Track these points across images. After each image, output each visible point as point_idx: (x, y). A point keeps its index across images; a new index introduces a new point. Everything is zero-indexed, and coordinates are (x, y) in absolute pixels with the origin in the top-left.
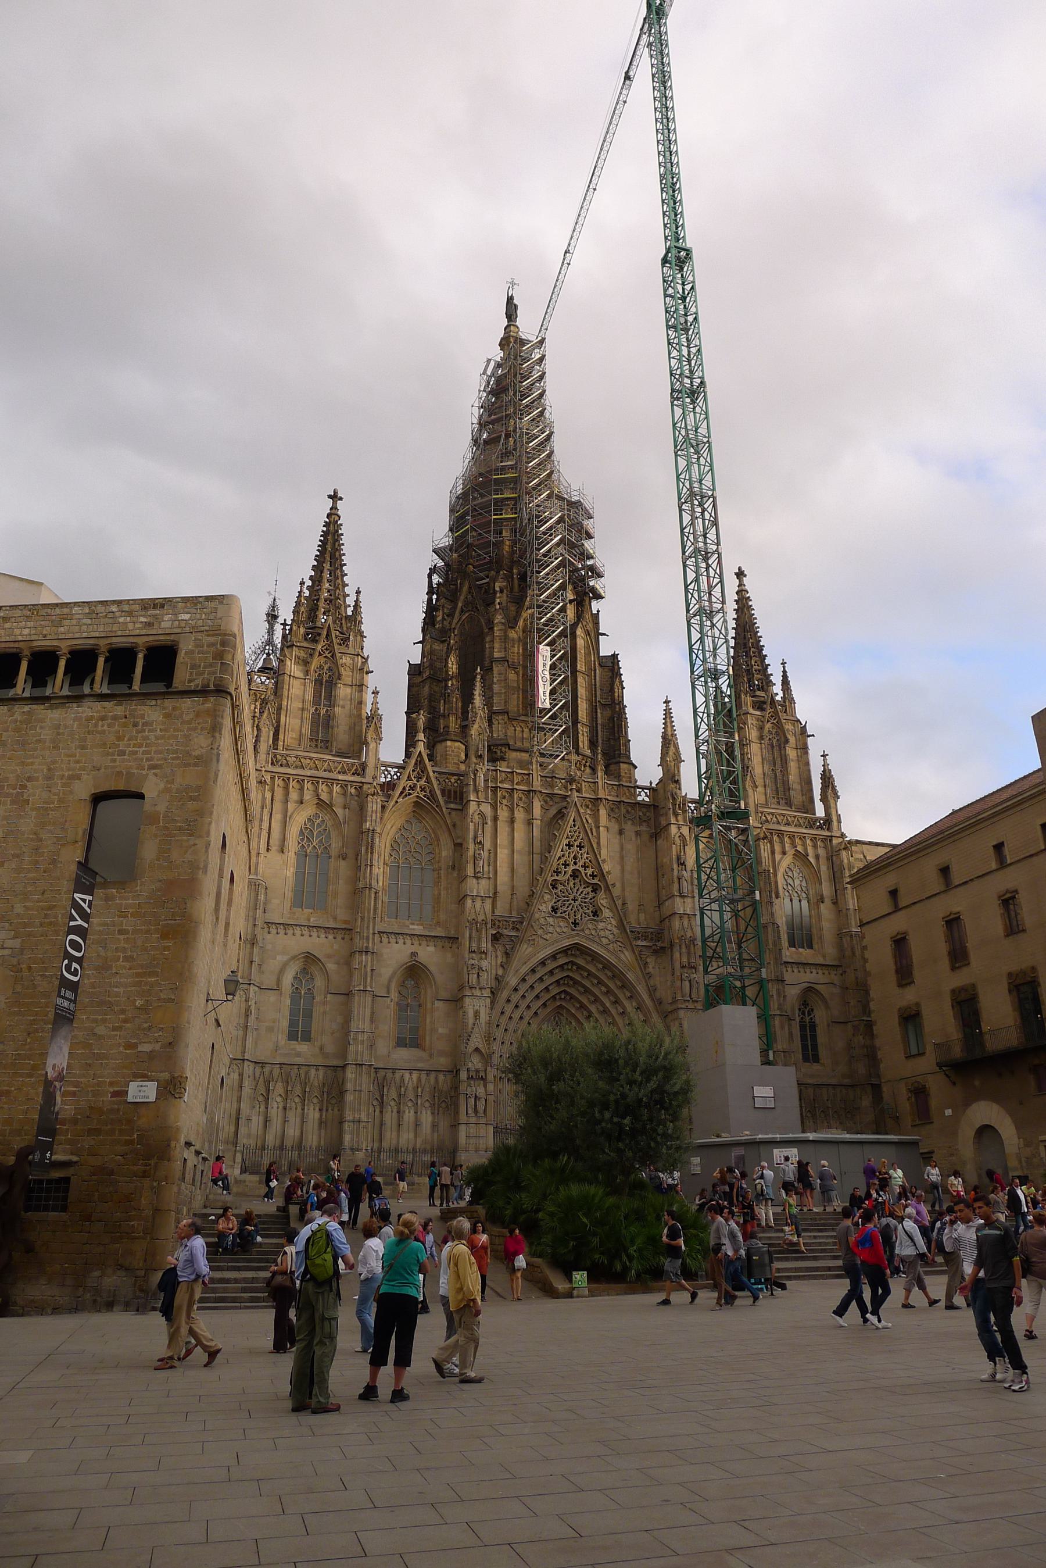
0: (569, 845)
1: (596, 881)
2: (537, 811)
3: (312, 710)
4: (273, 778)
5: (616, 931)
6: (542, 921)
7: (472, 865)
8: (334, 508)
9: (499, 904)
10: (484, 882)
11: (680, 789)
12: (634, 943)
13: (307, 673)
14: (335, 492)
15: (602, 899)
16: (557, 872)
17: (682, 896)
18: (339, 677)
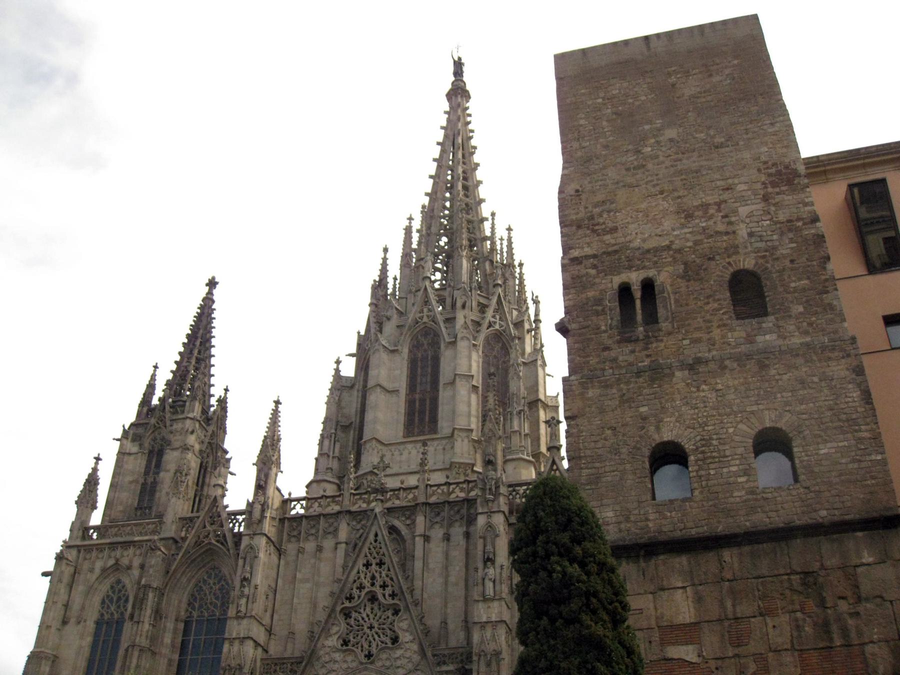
0: (367, 565)
1: (396, 601)
2: (343, 535)
3: (142, 481)
4: (79, 551)
5: (416, 658)
6: (327, 658)
7: (235, 605)
8: (210, 293)
9: (290, 646)
10: (245, 622)
11: (495, 470)
12: (438, 669)
13: (141, 445)
14: (214, 278)
15: (402, 625)
16: (350, 598)
17: (485, 600)
18: (169, 443)
